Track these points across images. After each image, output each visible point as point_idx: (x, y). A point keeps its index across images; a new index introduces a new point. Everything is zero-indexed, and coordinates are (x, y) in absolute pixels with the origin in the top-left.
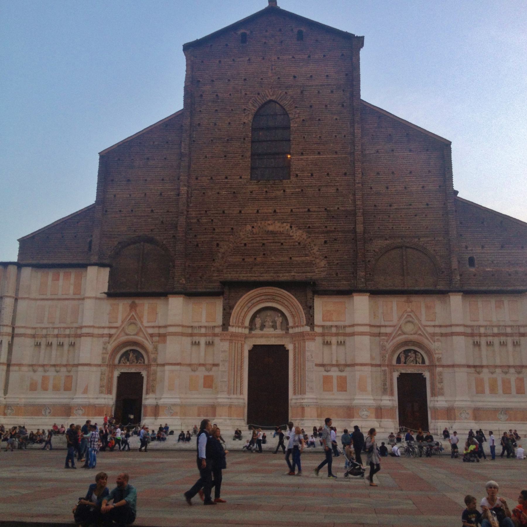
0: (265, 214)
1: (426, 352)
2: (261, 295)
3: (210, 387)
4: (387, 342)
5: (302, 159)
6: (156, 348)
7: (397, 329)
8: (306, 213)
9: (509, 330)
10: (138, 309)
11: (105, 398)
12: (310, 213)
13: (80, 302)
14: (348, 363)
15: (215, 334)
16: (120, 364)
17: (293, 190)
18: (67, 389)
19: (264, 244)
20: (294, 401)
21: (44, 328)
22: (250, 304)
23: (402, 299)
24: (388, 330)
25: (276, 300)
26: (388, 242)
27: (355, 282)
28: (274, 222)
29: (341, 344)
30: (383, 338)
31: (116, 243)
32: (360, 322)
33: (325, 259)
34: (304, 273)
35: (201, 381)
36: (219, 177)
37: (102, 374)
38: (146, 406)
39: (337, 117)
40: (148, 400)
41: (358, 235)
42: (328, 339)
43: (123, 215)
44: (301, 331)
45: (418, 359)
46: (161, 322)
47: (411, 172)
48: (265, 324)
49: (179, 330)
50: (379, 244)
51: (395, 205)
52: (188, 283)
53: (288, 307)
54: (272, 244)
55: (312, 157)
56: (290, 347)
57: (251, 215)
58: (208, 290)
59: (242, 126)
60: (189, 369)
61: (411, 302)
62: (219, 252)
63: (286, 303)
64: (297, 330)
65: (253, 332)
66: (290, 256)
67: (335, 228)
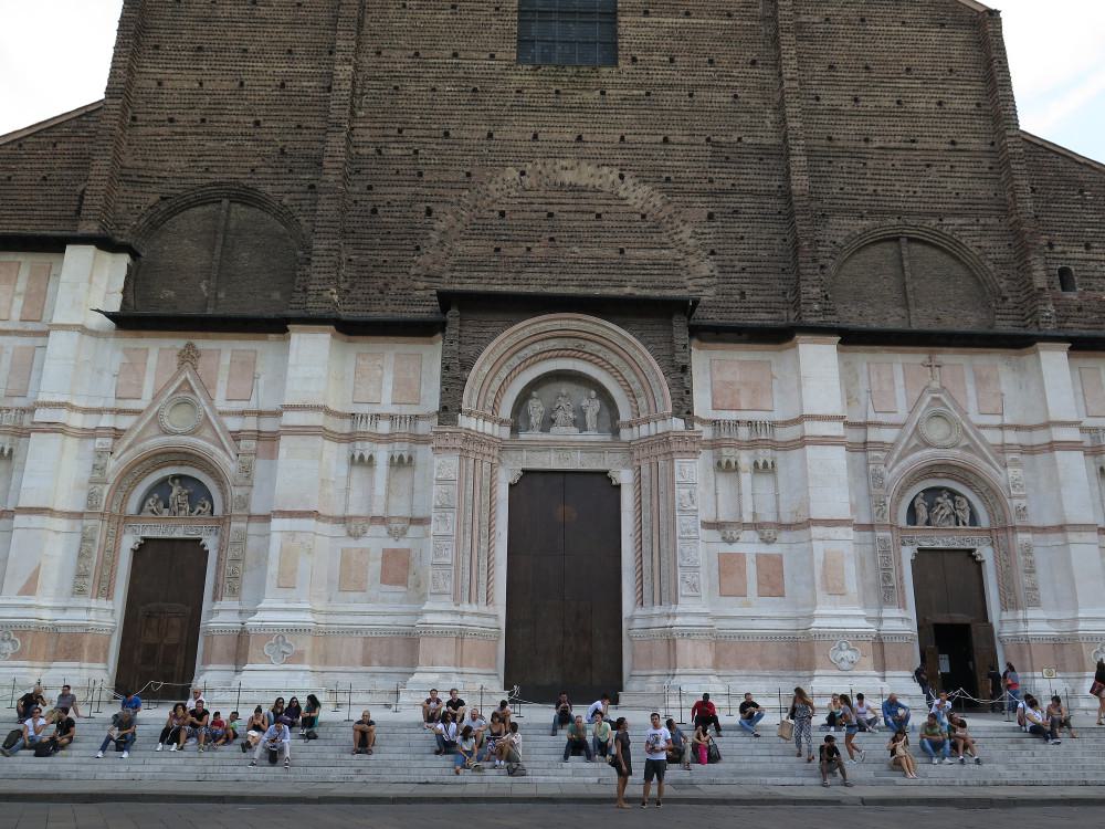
1: (981, 495)
3: (402, 581)
5: (645, 25)
6: (247, 470)
7: (909, 433)
8: (658, 146)
11: (88, 609)
12: (670, 147)
13: (40, 341)
14: (786, 519)
16: (142, 515)
17: (625, 92)
19: (551, 215)
20: (638, 623)
22: (515, 361)
23: (915, 358)
24: (888, 435)
25: (586, 353)
26: (865, 222)
28: (578, 164)
30: (876, 454)
31: (154, 199)
33: (712, 257)
35: (375, 567)
37: (84, 540)
38: (210, 636)
40: (219, 616)
41: (797, 198)
42: (727, 454)
43: (179, 130)
45: (959, 513)
46: (264, 400)
47: (908, 70)
48: (553, 417)
49: (316, 419)
50: (842, 228)
51: (877, 138)
54: (572, 215)
55: (670, 20)
56: (624, 477)
60: (340, 530)
61: (939, 366)
62: (433, 229)
63: (615, 360)
64: (644, 430)
65: (523, 436)
67: (733, 185)
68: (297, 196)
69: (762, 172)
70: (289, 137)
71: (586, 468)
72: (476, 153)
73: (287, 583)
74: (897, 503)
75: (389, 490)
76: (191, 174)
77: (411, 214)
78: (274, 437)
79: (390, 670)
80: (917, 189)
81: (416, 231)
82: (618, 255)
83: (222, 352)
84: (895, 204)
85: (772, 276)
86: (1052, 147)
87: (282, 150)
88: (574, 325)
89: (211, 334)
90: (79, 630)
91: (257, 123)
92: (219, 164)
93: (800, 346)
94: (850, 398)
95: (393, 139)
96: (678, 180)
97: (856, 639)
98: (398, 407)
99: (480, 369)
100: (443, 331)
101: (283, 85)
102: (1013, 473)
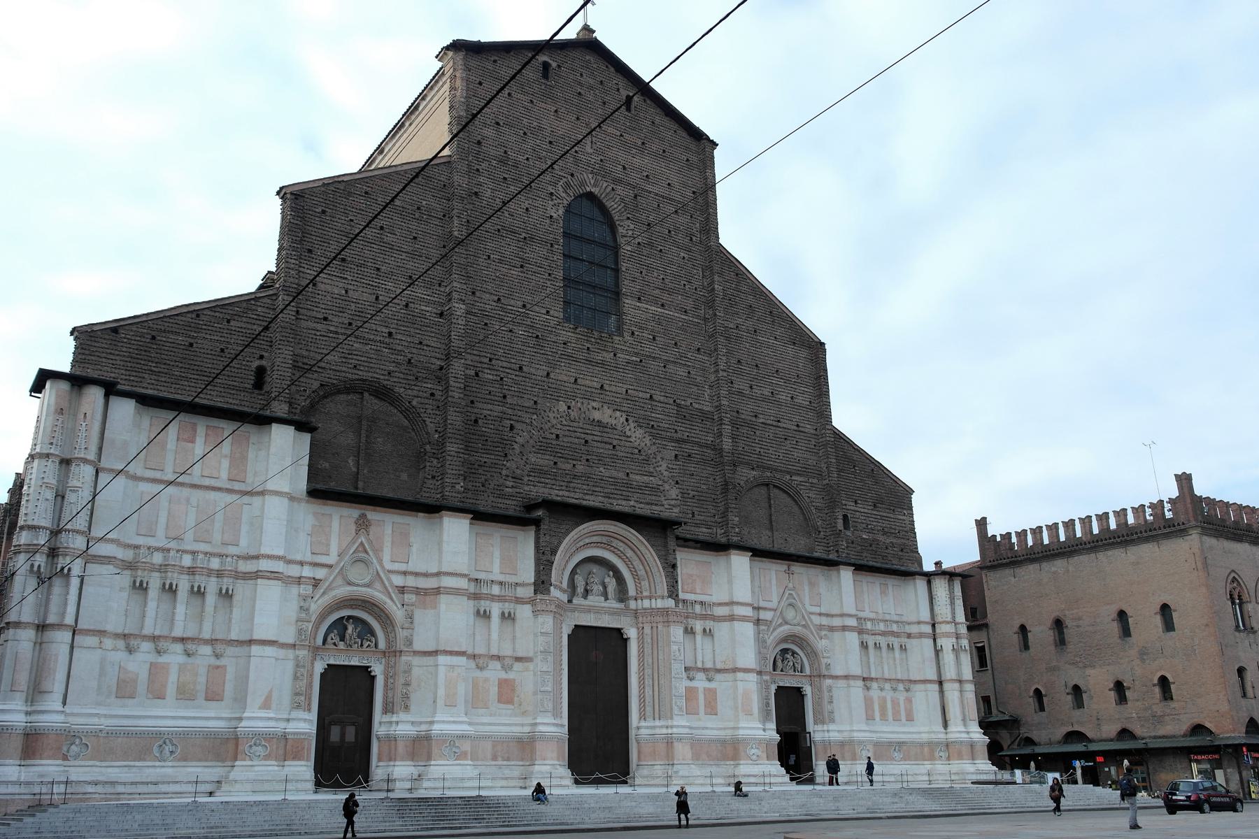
0: (587, 389)
1: (807, 655)
3: (510, 701)
6: (410, 617)
7: (778, 614)
9: (895, 628)
10: (373, 530)
14: (719, 666)
16: (327, 646)
18: (213, 696)
19: (586, 442)
21: (157, 549)
26: (755, 473)
29: (707, 633)
31: (316, 385)
32: (741, 600)
33: (677, 486)
34: (648, 504)
35: (494, 690)
36: (512, 302)
37: (297, 666)
39: (686, 256)
43: (332, 328)
45: (796, 665)
49: (462, 583)
51: (761, 416)
55: (653, 308)
56: (631, 633)
57: (566, 384)
59: (548, 221)
60: (472, 664)
62: (516, 443)
63: (629, 553)
64: (646, 603)
66: (628, 471)
67: (688, 436)
68: (423, 401)
69: (703, 430)
70: (414, 351)
71: (611, 626)
72: (540, 387)
73: (451, 705)
76: (344, 369)
77: (501, 428)
79: (509, 763)
80: (780, 454)
81: (505, 442)
82: (626, 478)
83: (387, 523)
84: (769, 463)
85: (708, 503)
86: (843, 436)
87: (410, 360)
88: (612, 528)
89: (378, 508)
90: (302, 737)
91: (390, 334)
92: (363, 363)
95: (486, 366)
96: (658, 428)
97: (760, 741)
98: (503, 576)
101: (407, 306)
102: (824, 642)
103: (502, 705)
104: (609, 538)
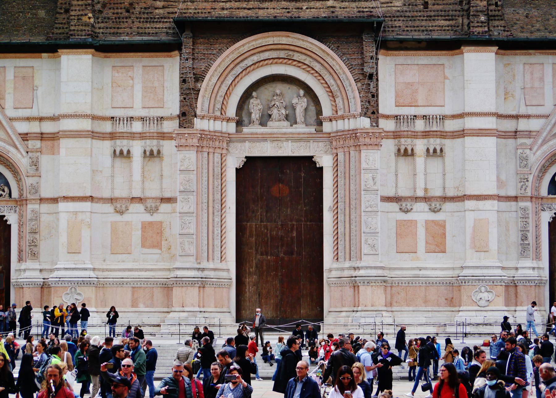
2: (263, 48)
3: (158, 246)
4: (531, 149)
6: (35, 164)
14: (450, 194)
15: (164, 133)
20: (334, 274)
22: (238, 69)
24: (534, 125)
25: (295, 60)
27: (466, 21)
35: (137, 236)
42: (406, 143)
44: (352, 127)
48: (270, 112)
49: (86, 125)
52: (98, 22)
53: (320, 76)
58: (145, 38)
60: (108, 208)
63: (317, 67)
64: (340, 125)
65: (246, 130)
74: (540, 178)
75: (143, 176)
78: (54, 137)
88: (284, 40)
93: (465, 54)
94: (507, 95)
97: (492, 282)
98: (147, 110)
99: (210, 80)
100: (180, 49)
103: (146, 249)
104: (286, 52)
